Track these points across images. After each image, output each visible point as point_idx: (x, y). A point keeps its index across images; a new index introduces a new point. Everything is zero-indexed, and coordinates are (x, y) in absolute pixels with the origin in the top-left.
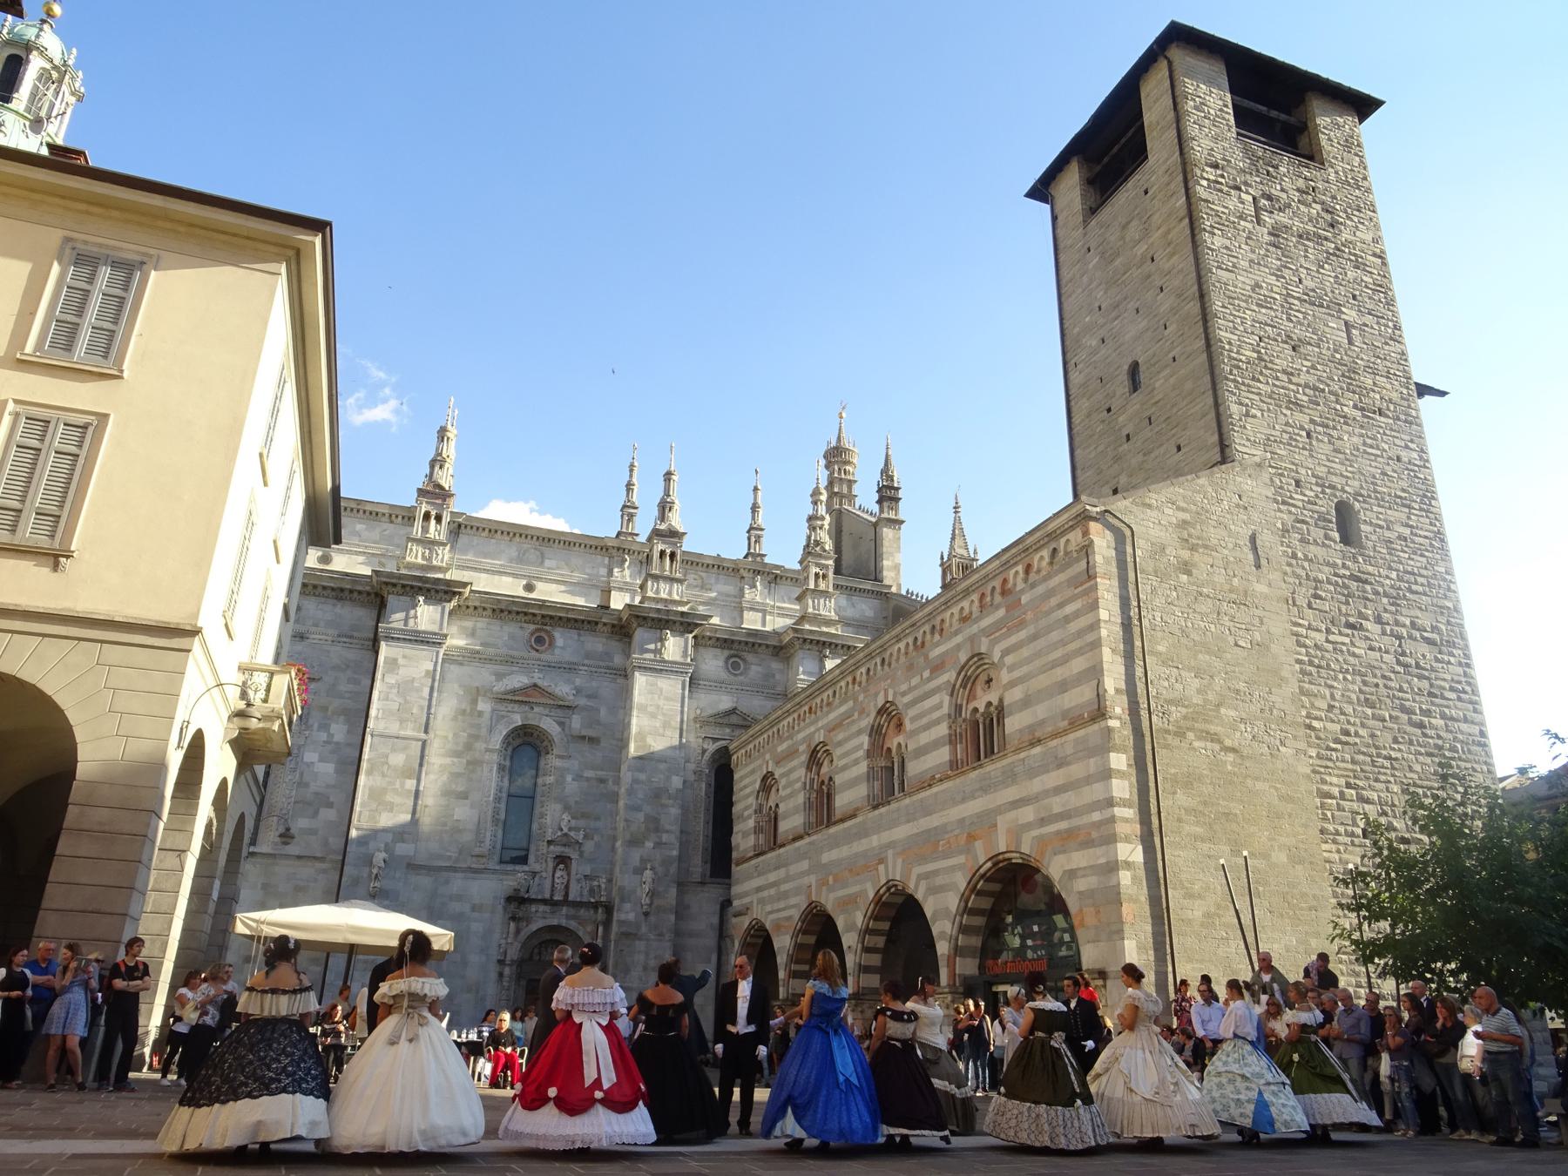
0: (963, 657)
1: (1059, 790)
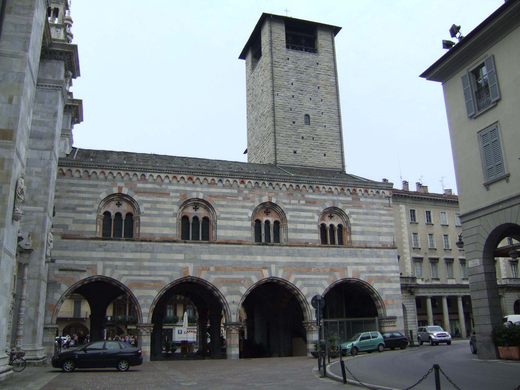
0: (328, 205)
1: (377, 264)
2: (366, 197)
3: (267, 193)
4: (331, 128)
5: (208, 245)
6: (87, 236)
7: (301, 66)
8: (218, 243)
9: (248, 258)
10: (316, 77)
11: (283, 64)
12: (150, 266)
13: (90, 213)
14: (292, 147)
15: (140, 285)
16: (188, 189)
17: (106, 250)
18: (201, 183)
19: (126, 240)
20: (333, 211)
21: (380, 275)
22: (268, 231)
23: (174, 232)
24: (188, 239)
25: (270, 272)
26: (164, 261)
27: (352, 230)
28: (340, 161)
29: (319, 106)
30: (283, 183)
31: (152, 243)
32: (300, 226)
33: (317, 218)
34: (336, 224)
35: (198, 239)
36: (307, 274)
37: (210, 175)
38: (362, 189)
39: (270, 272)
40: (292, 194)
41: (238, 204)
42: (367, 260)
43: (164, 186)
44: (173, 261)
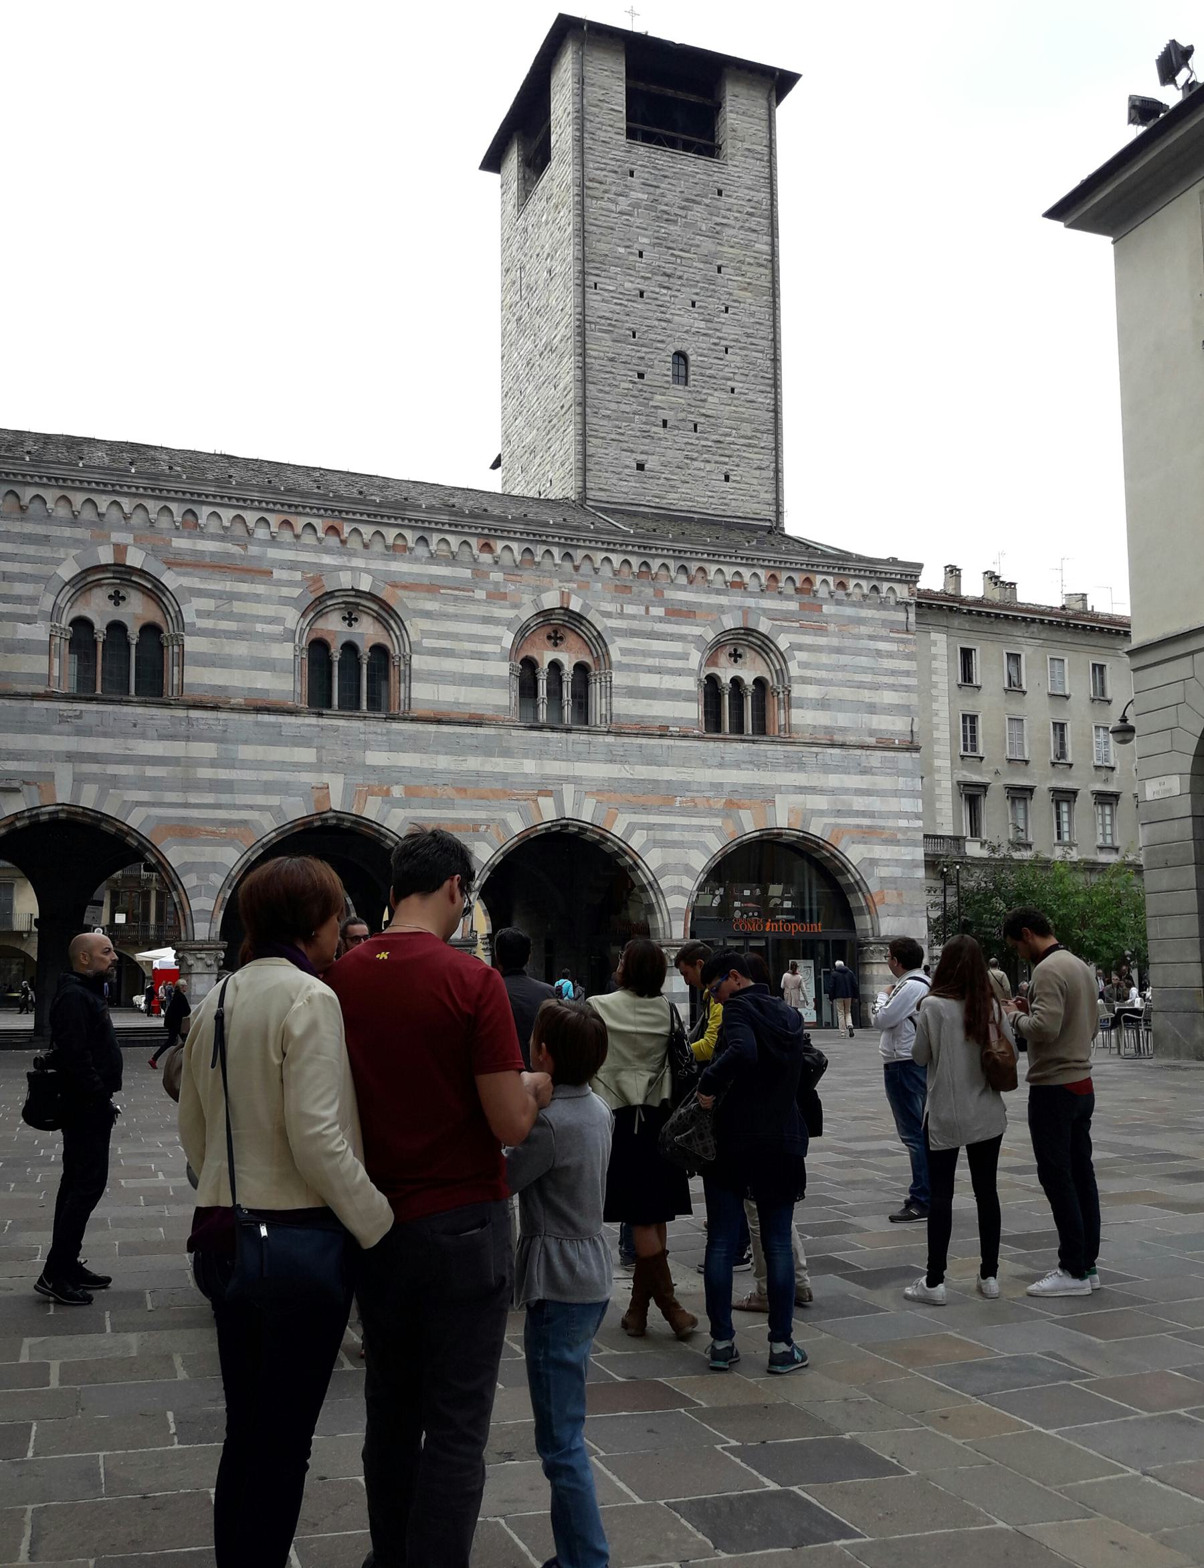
0: (729, 622)
1: (859, 792)
2: (839, 603)
3: (556, 583)
4: (751, 397)
5: (387, 725)
6: (20, 688)
7: (669, 198)
8: (414, 720)
9: (500, 765)
10: (715, 234)
11: (614, 188)
12: (217, 781)
13: (29, 620)
14: (632, 451)
15: (186, 832)
16: (327, 560)
17: (80, 732)
18: (366, 546)
19: (144, 704)
20: (743, 640)
21: (866, 822)
22: (558, 687)
23: (287, 684)
24: (329, 705)
25: (560, 805)
26: (259, 765)
27: (793, 695)
28: (770, 497)
29: (718, 326)
30: (604, 555)
31: (222, 715)
32: (647, 681)
33: (695, 658)
34: (748, 678)
35: (357, 707)
36: (661, 813)
37: (392, 521)
38: (830, 579)
39: (560, 805)
40: (626, 589)
41: (472, 610)
42: (834, 780)
43: (254, 550)
44: (283, 766)
